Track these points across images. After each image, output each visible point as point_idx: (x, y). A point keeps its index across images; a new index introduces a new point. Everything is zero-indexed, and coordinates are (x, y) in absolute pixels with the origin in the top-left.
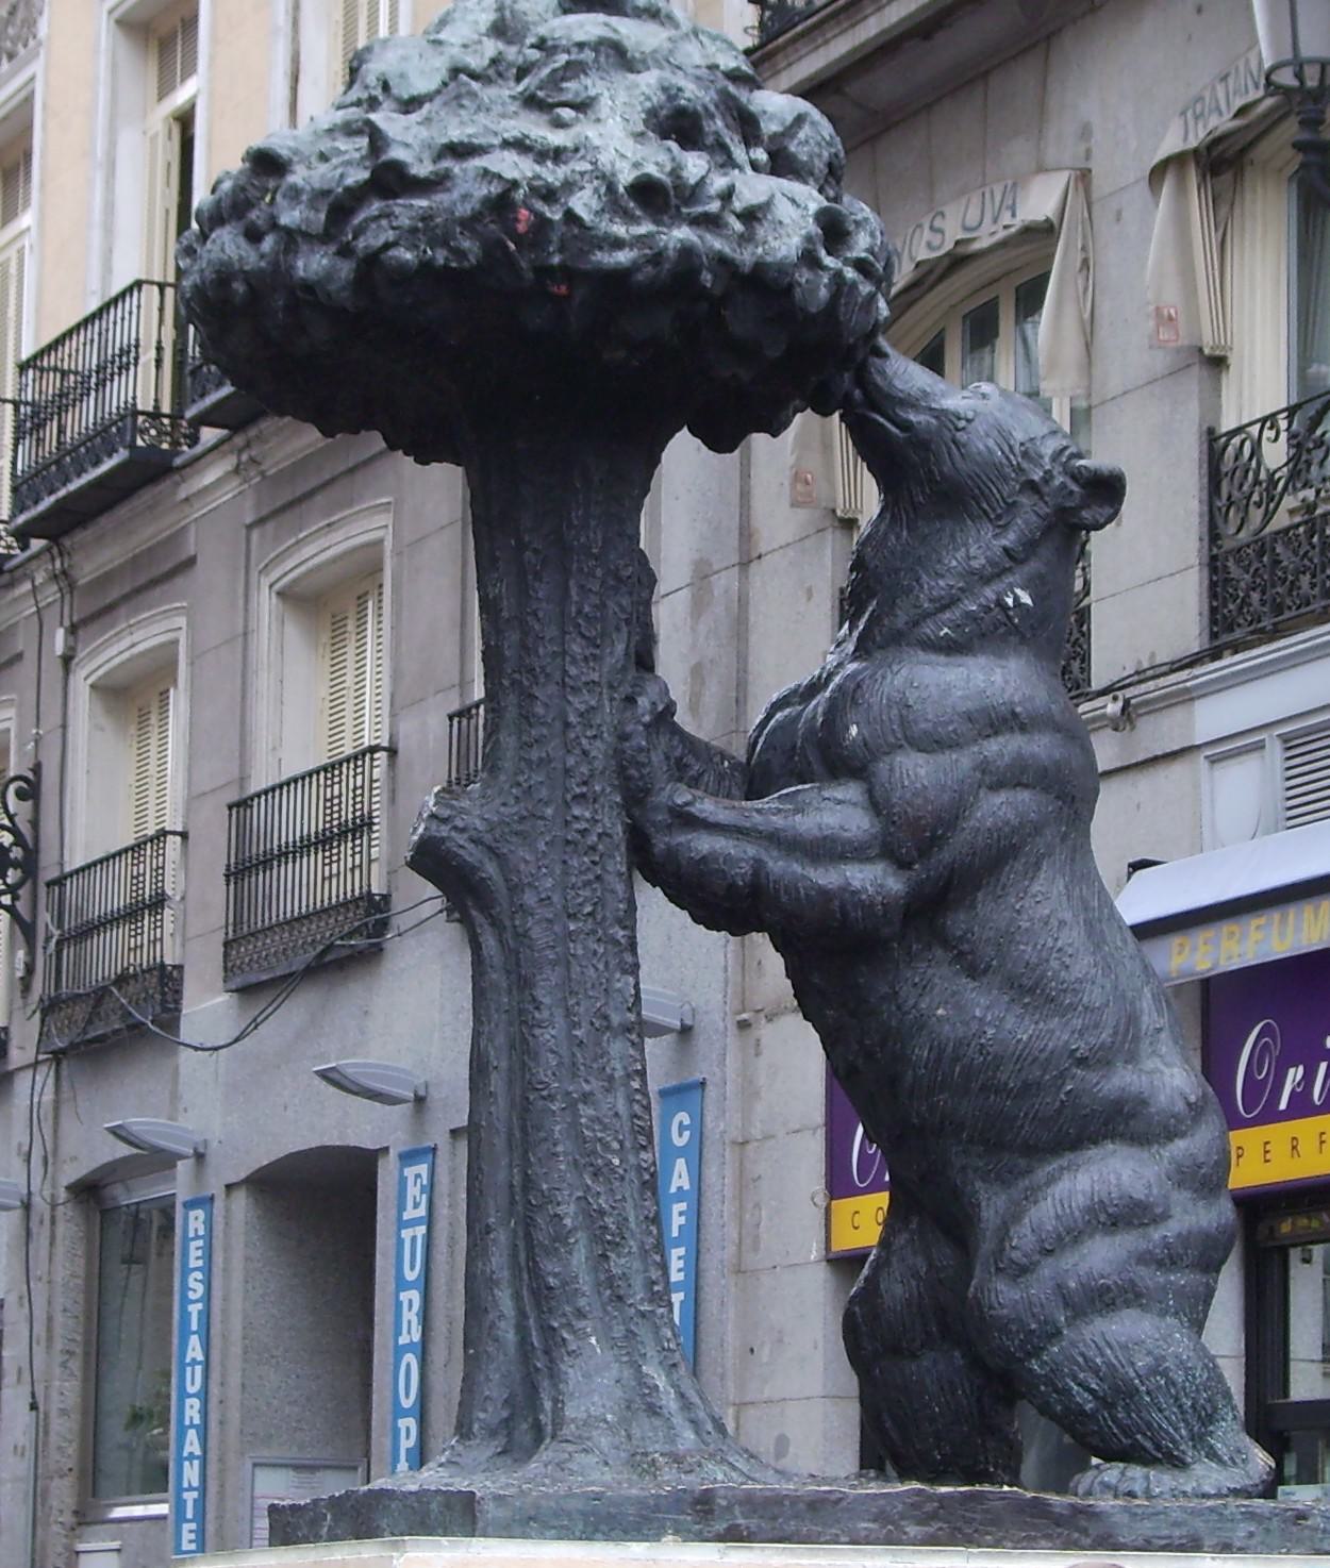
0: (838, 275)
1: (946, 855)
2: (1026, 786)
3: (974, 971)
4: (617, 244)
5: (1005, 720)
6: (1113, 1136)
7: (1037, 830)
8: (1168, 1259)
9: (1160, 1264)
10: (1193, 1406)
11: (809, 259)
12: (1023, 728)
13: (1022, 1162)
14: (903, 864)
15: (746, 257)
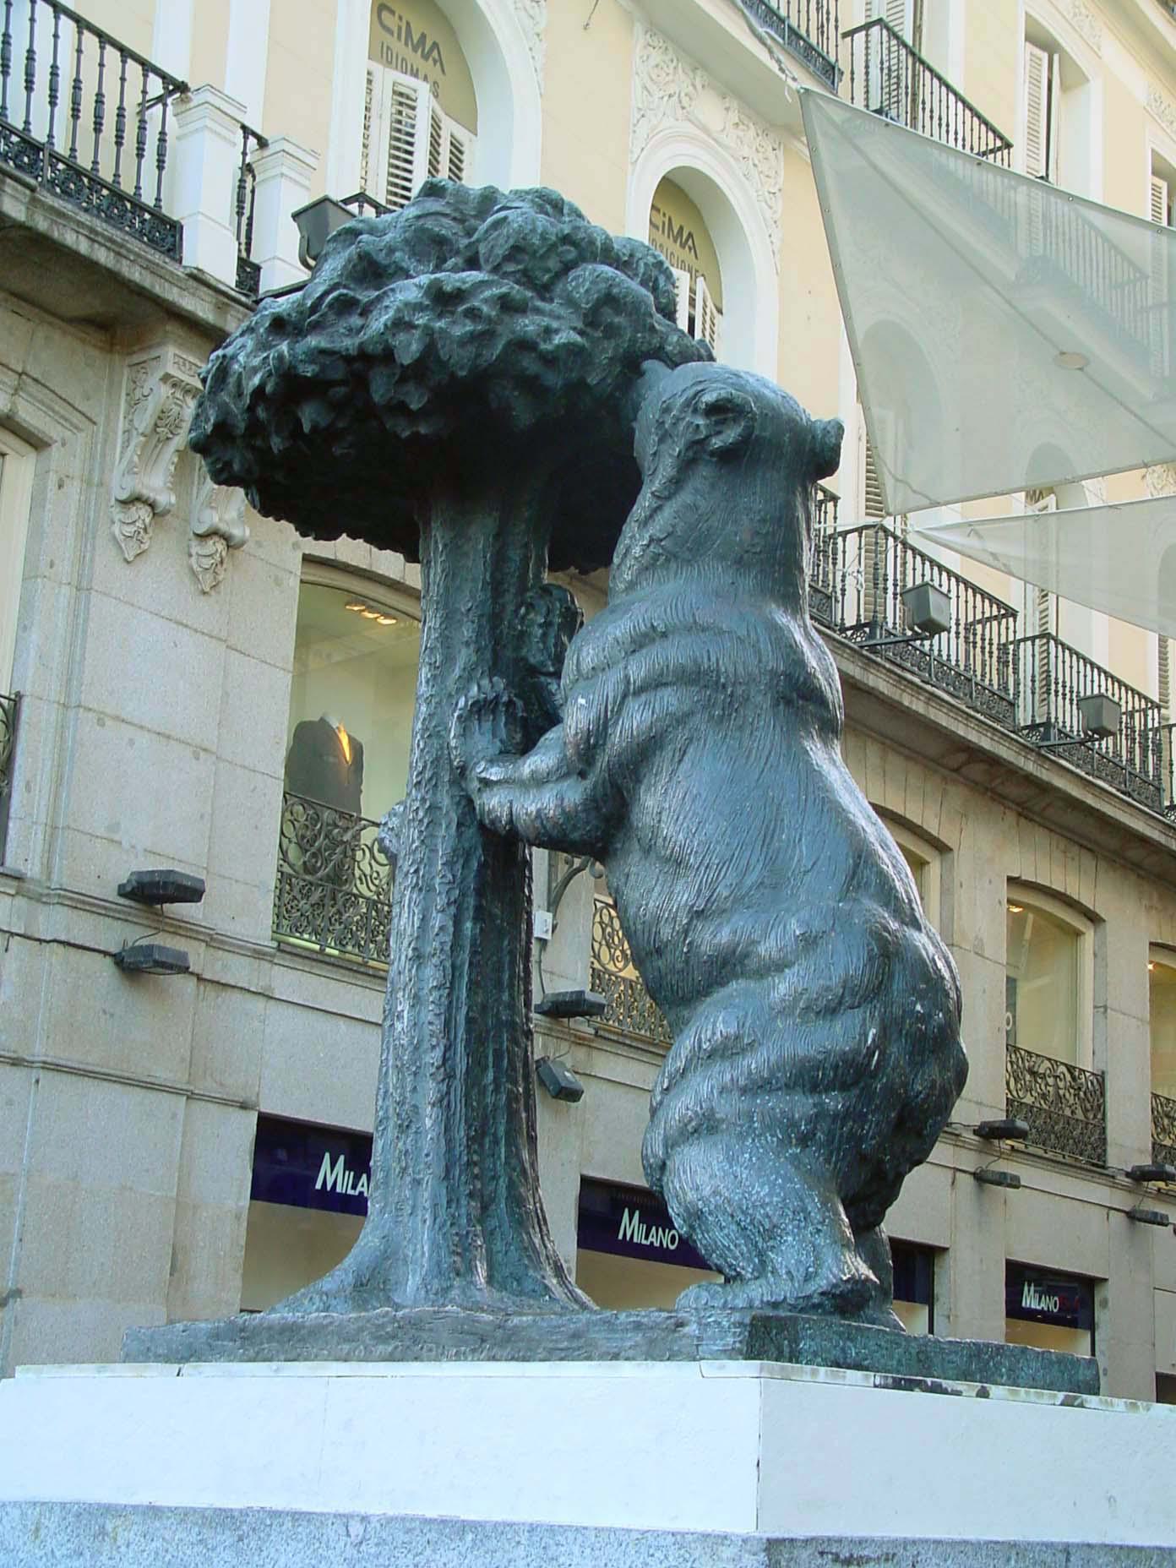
0: (428, 331)
1: (602, 761)
2: (666, 684)
3: (647, 851)
4: (255, 370)
5: (645, 635)
6: (736, 977)
7: (681, 720)
8: (758, 1086)
9: (744, 1091)
10: (752, 1222)
11: (400, 324)
12: (664, 635)
13: (686, 1013)
14: (582, 775)
15: (349, 344)
